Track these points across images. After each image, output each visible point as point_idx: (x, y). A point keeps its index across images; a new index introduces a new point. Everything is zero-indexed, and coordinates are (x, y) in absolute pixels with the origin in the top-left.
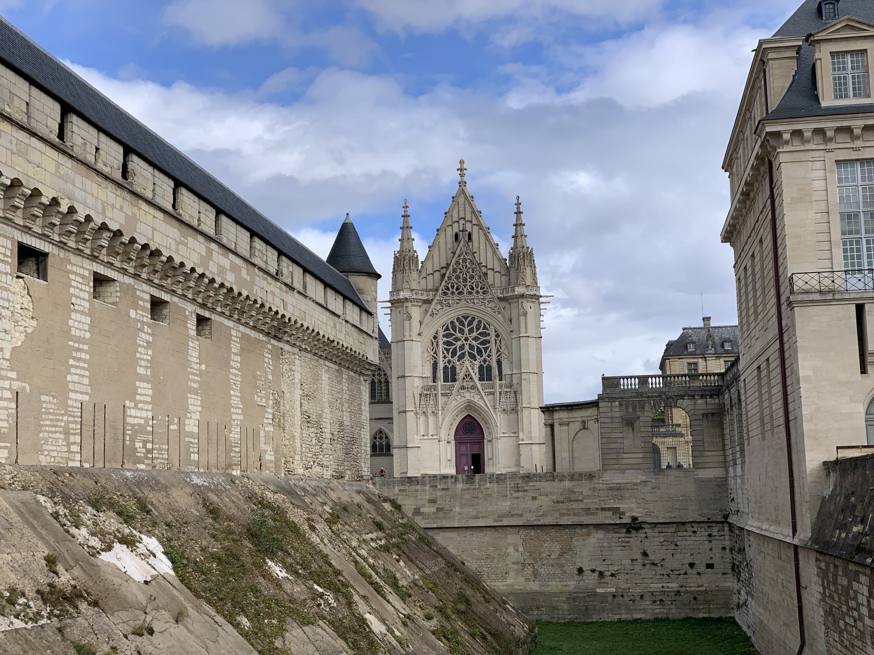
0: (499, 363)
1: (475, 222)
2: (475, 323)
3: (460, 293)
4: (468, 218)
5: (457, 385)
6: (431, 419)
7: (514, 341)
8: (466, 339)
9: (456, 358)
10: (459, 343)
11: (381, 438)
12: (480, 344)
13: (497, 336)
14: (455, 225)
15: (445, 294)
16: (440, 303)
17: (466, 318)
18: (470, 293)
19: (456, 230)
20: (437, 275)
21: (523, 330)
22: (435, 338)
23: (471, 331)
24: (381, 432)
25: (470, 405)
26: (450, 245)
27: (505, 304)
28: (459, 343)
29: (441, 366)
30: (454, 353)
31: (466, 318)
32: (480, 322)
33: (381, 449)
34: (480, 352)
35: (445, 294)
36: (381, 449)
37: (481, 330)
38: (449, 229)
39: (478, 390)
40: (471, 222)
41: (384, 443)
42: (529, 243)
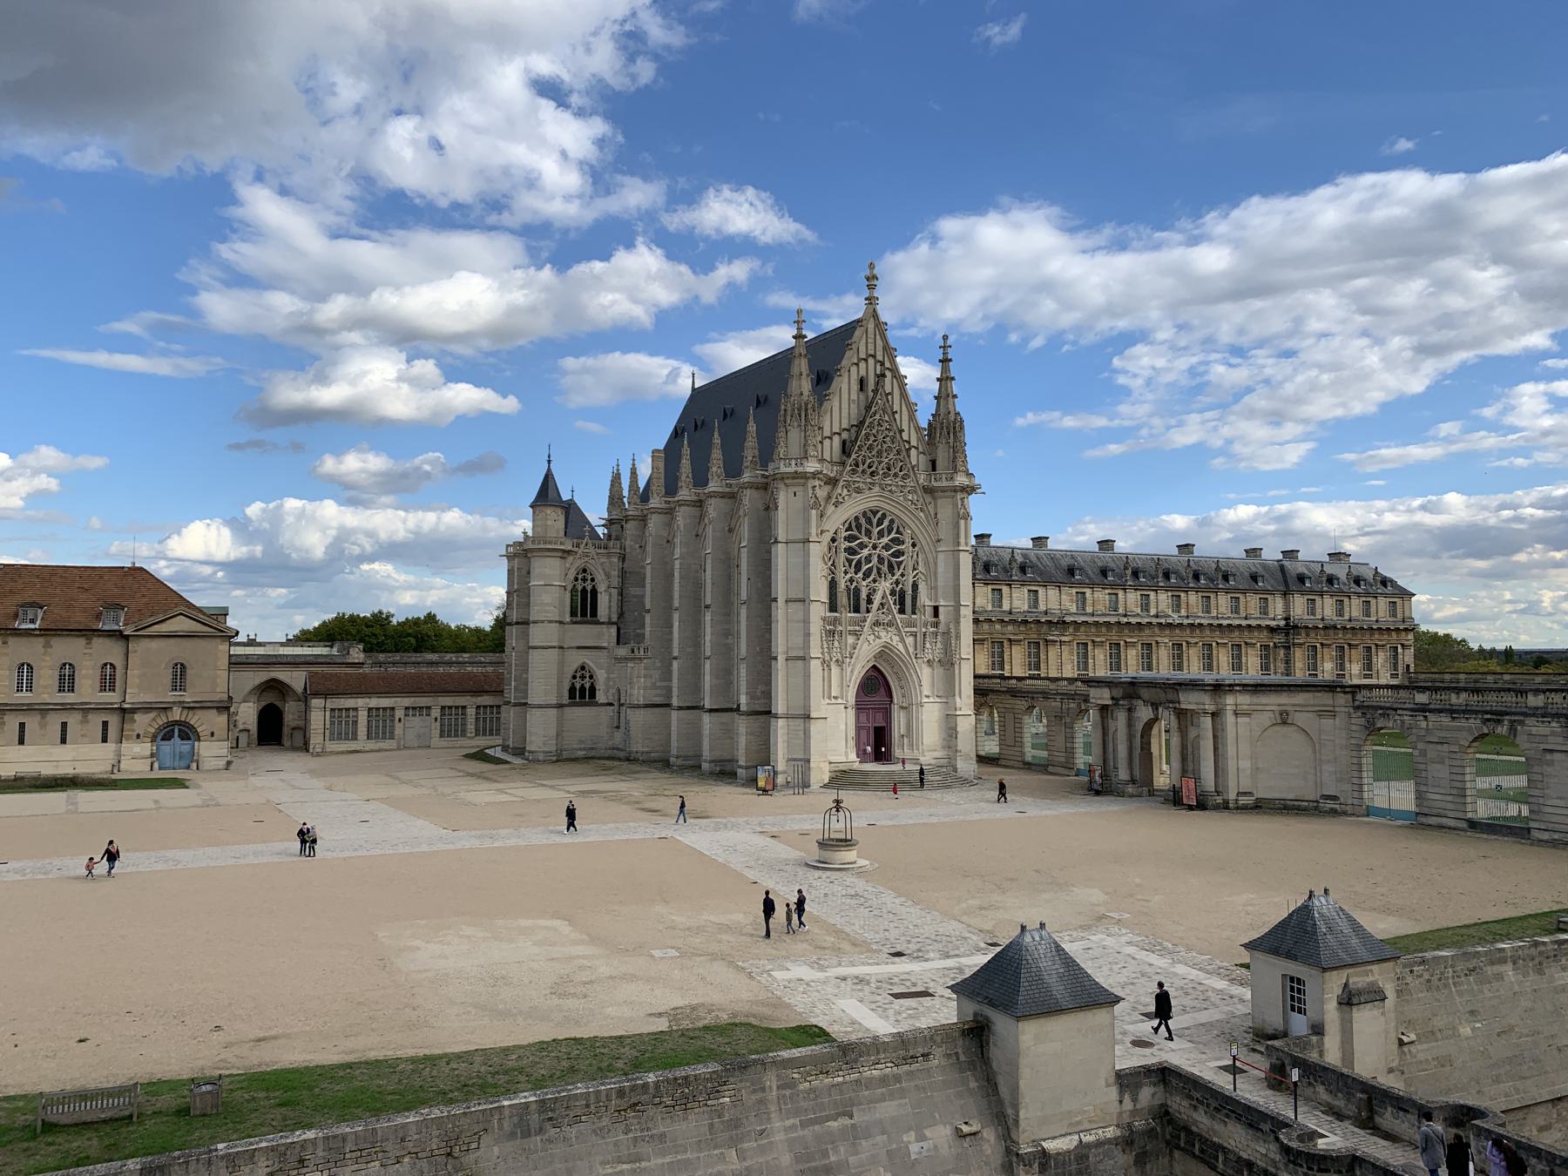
0: (915, 586)
1: (887, 365)
2: (886, 523)
3: (872, 474)
4: (880, 358)
5: (871, 617)
6: (835, 670)
7: (941, 556)
8: (875, 547)
9: (860, 575)
10: (865, 552)
11: (583, 677)
12: (893, 555)
13: (914, 545)
14: (863, 365)
15: (854, 472)
16: (847, 487)
17: (875, 513)
18: (885, 475)
19: (863, 373)
20: (836, 439)
21: (962, 540)
22: (833, 540)
23: (881, 535)
24: (583, 668)
25: (885, 653)
26: (854, 396)
27: (928, 498)
28: (865, 552)
29: (842, 585)
30: (858, 568)
31: (875, 513)
32: (892, 521)
33: (582, 696)
34: (891, 567)
35: (854, 472)
36: (582, 696)
37: (893, 535)
38: (854, 369)
39: (897, 628)
40: (882, 364)
41: (587, 686)
42: (960, 406)
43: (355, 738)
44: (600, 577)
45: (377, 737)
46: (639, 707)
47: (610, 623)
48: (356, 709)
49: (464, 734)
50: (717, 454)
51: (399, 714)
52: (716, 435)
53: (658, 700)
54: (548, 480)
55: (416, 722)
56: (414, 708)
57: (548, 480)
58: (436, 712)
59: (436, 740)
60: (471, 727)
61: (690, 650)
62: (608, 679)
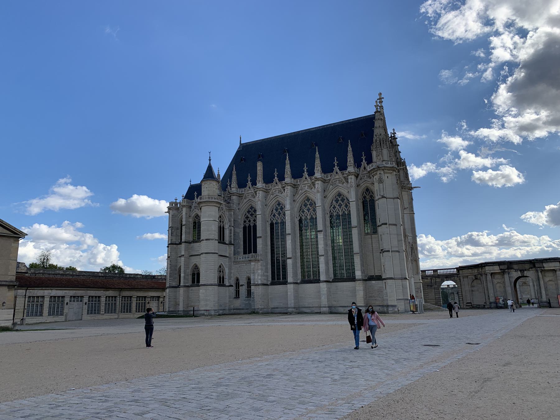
7: (405, 215)
43: (41, 315)
44: (226, 221)
45: (53, 314)
46: (258, 285)
47: (230, 244)
48: (43, 297)
49: (99, 313)
50: (318, 162)
51: (67, 300)
52: (317, 153)
53: (265, 282)
54: (210, 168)
55: (76, 305)
56: (74, 297)
57: (210, 168)
58: (86, 300)
59: (86, 317)
60: (103, 308)
61: (294, 254)
62: (230, 273)
